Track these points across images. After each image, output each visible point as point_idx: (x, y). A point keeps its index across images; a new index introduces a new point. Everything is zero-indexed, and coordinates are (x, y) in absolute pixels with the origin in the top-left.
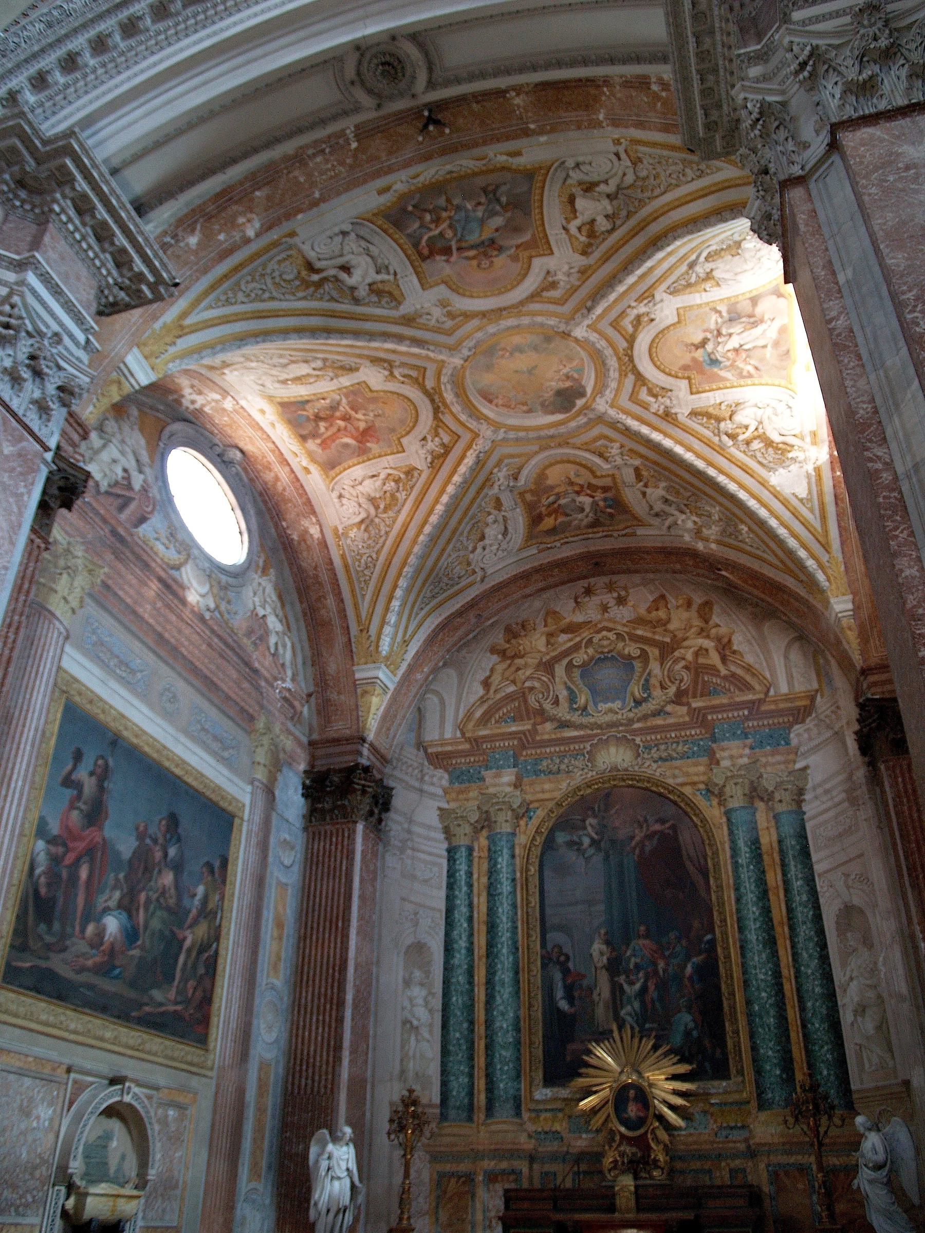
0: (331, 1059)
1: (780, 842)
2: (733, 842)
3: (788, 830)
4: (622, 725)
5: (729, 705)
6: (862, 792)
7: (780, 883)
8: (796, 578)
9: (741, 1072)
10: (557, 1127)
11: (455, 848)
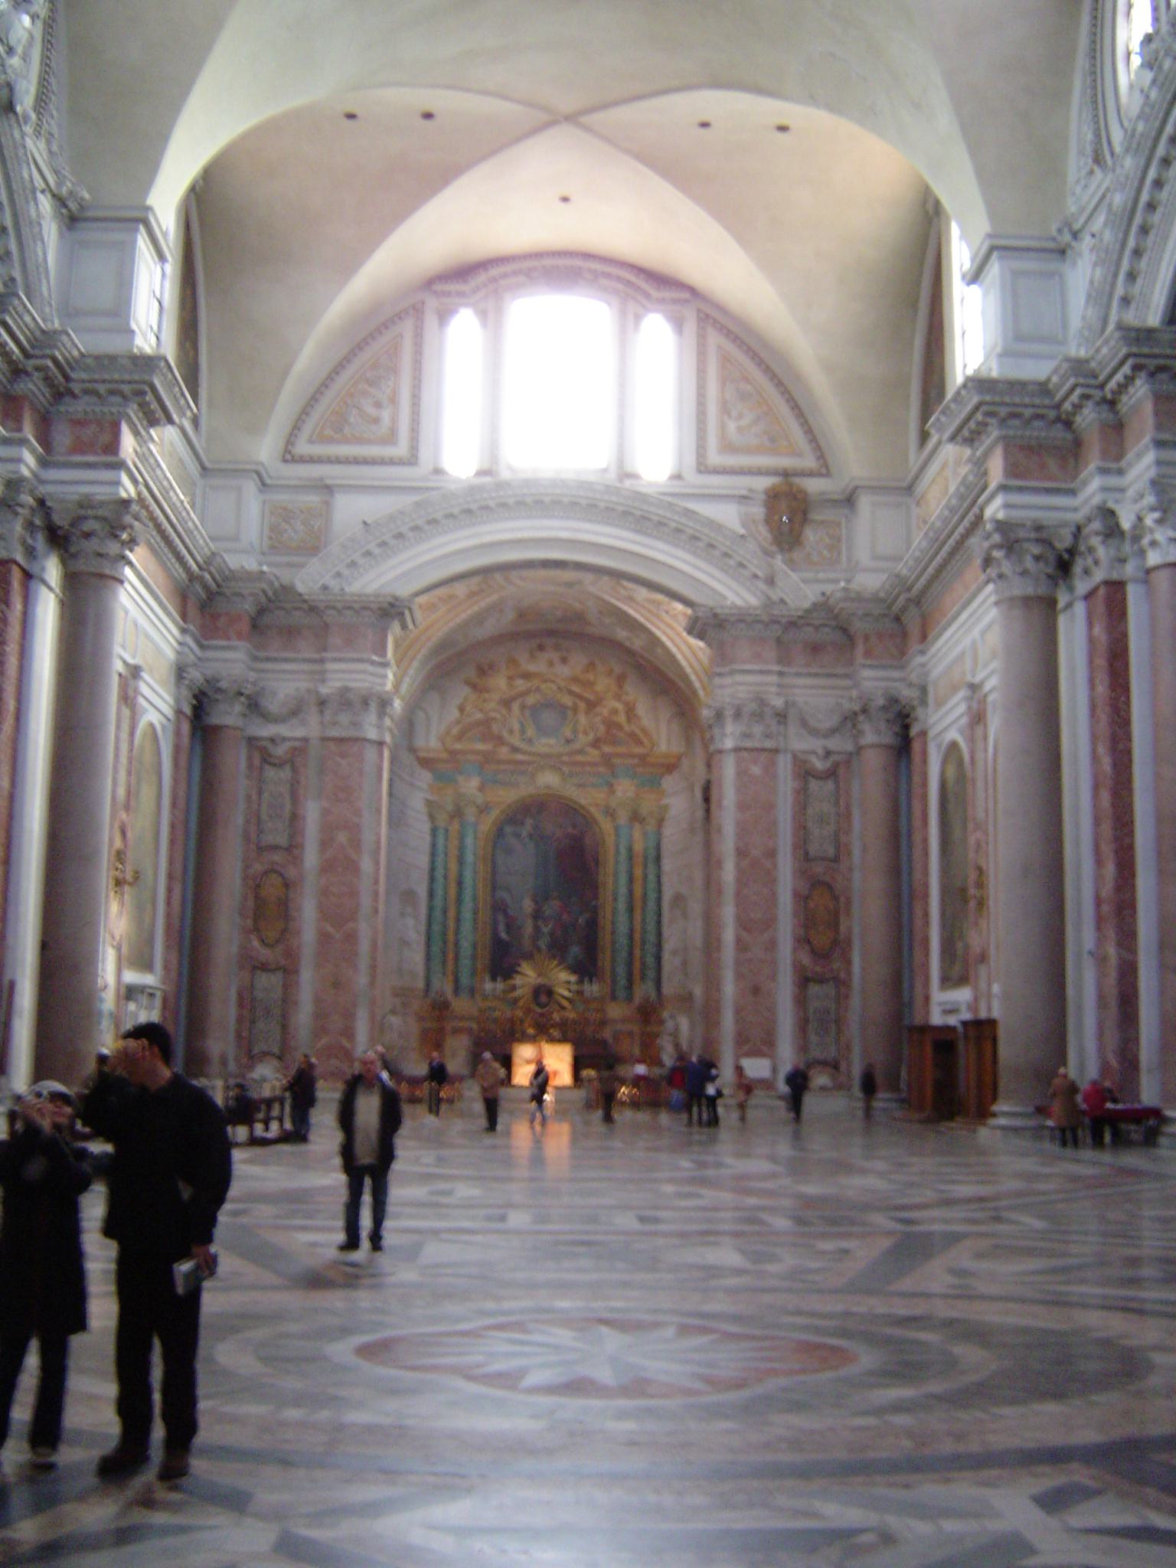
1: (645, 849)
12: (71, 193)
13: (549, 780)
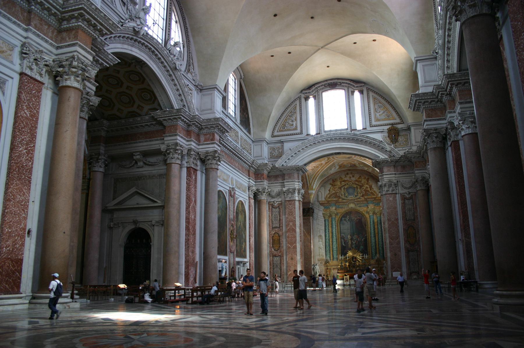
2: (370, 221)
3: (379, 219)
9: (370, 254)
12: (198, 84)
13: (352, 205)
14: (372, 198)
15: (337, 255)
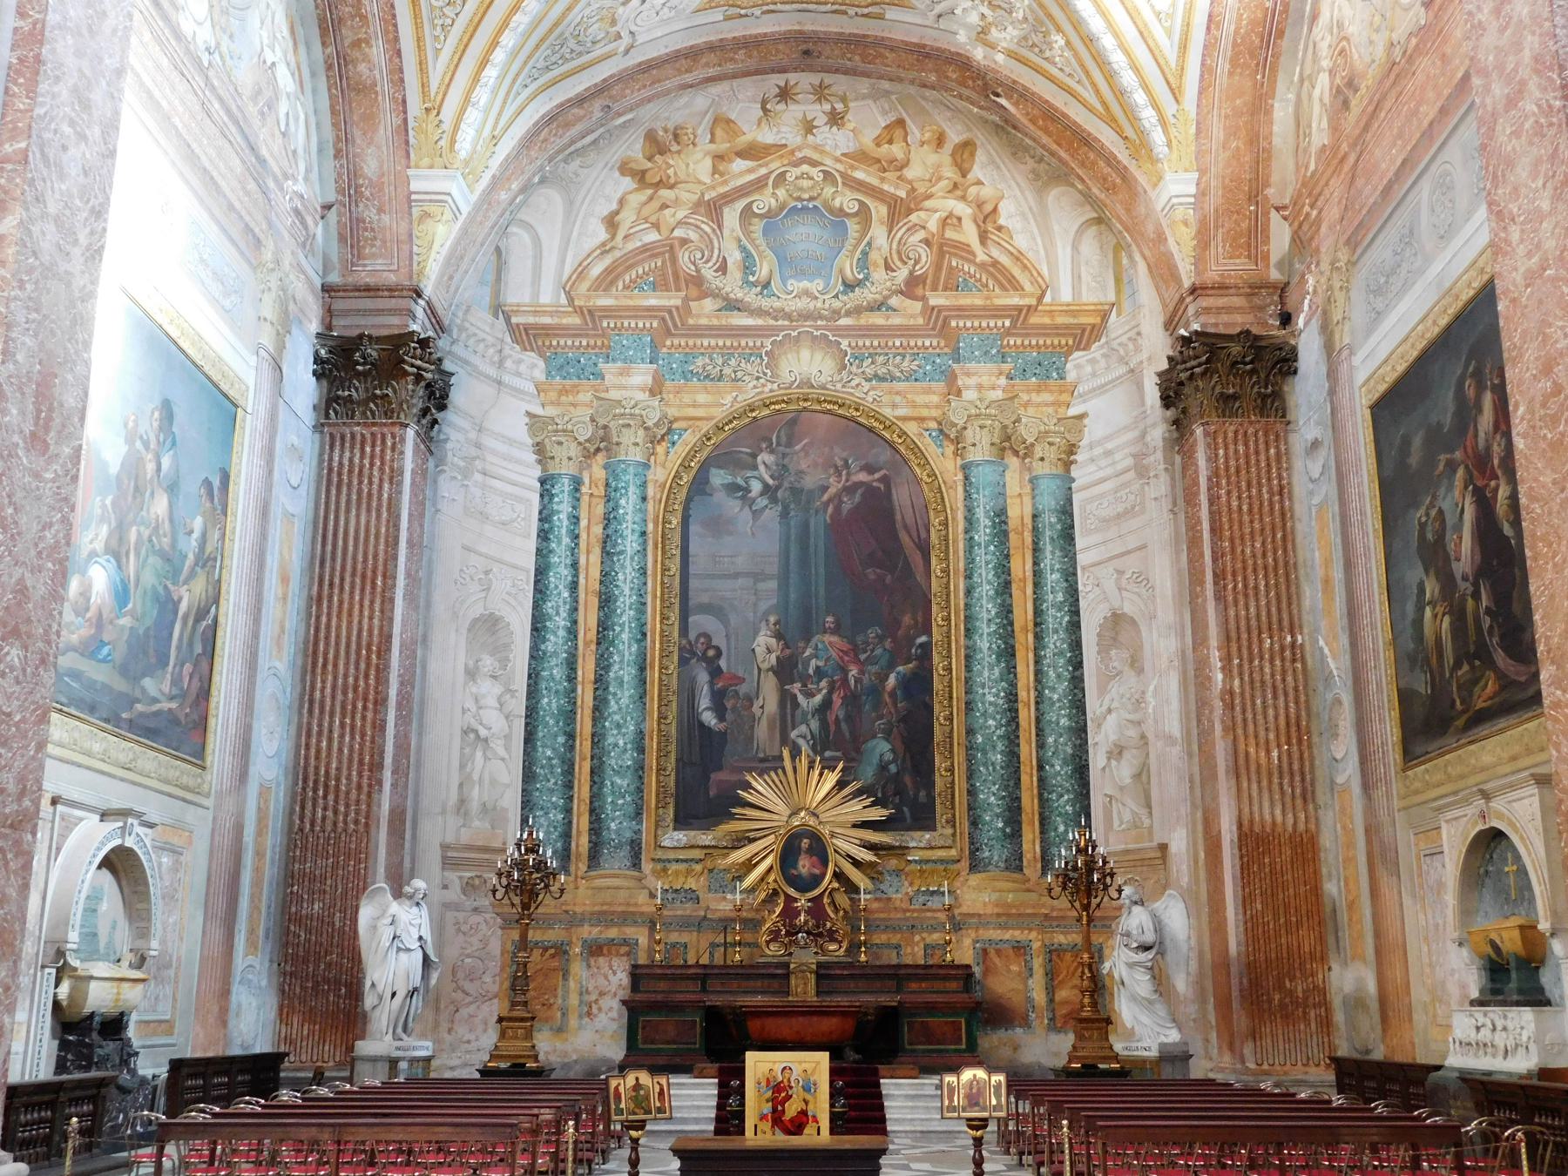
0: (365, 781)
1: (1035, 516)
2: (970, 510)
3: (1048, 502)
4: (821, 317)
5: (984, 308)
6: (1157, 459)
7: (1029, 574)
8: (1119, 131)
9: (952, 822)
10: (691, 883)
11: (552, 477)
14: (998, 312)
15: (638, 814)
